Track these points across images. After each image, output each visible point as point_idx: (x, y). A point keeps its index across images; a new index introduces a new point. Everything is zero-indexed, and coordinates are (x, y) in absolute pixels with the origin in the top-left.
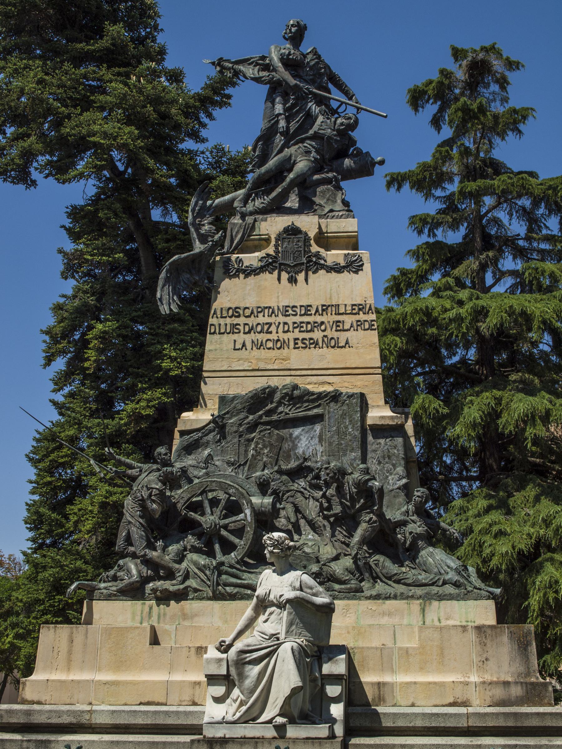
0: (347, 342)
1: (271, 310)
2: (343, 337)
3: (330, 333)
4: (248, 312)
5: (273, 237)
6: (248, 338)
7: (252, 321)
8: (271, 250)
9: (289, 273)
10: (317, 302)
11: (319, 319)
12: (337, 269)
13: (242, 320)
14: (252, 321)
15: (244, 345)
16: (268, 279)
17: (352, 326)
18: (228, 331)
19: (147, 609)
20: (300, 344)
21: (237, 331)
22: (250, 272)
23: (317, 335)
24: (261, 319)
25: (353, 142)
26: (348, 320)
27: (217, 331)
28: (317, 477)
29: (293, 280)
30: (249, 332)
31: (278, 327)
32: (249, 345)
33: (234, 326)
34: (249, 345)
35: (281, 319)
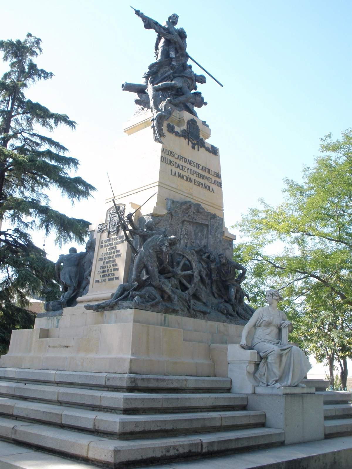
0: (213, 190)
1: (185, 160)
2: (212, 186)
3: (208, 184)
4: (176, 156)
5: (186, 121)
6: (177, 170)
7: (178, 161)
8: (185, 127)
9: (192, 143)
10: (202, 164)
11: (203, 173)
12: (207, 149)
13: (173, 159)
14: (178, 161)
15: (175, 173)
16: (183, 141)
17: (214, 182)
18: (169, 163)
19: (163, 319)
20: (196, 184)
21: (172, 165)
22: (177, 134)
23: (202, 181)
24: (181, 163)
25: (195, 88)
26: (214, 179)
27: (164, 161)
28: (208, 257)
29: (193, 148)
30: (177, 167)
31: (188, 170)
32: (177, 174)
33: (171, 162)
34: (177, 174)
35: (188, 166)
